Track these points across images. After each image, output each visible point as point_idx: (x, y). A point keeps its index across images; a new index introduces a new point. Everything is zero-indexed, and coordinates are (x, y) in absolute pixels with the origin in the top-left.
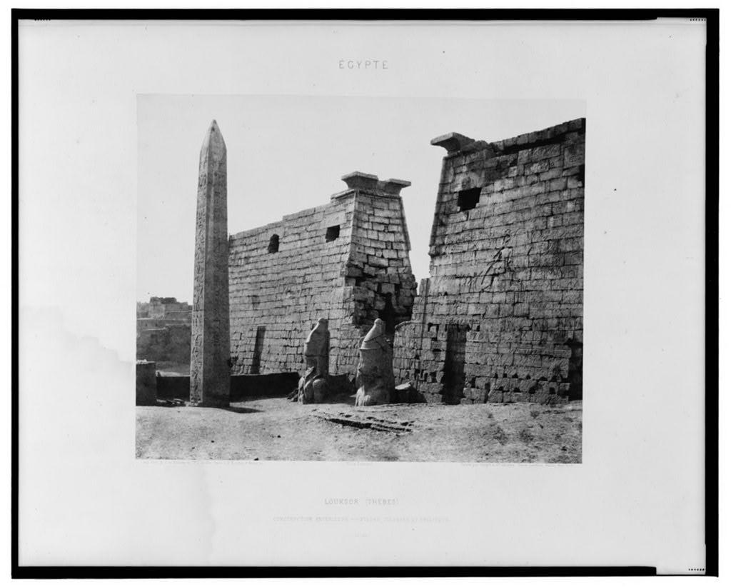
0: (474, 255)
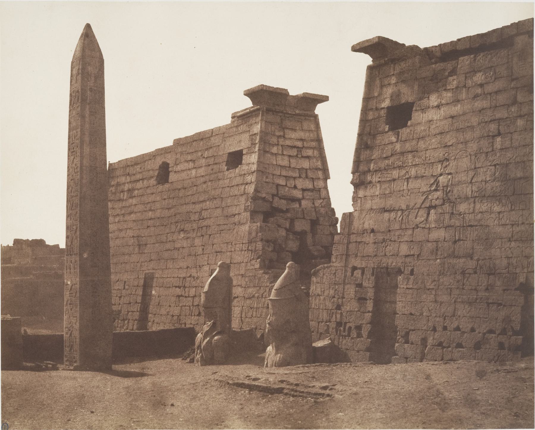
0: (406, 183)
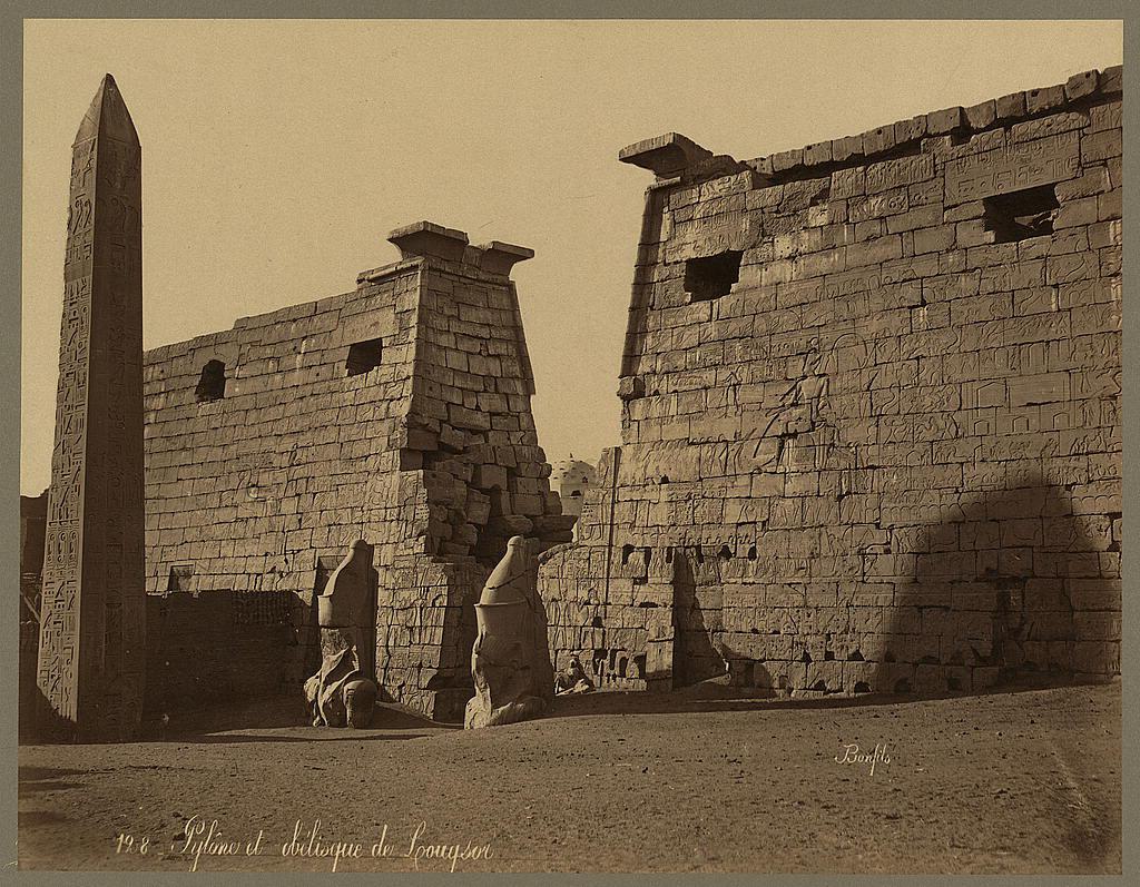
0: (731, 393)
